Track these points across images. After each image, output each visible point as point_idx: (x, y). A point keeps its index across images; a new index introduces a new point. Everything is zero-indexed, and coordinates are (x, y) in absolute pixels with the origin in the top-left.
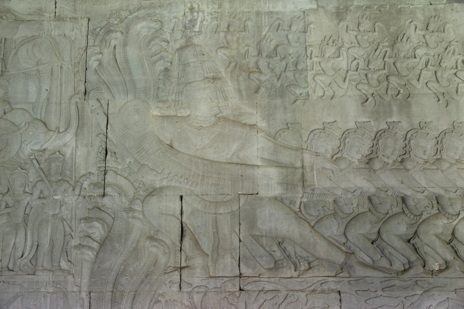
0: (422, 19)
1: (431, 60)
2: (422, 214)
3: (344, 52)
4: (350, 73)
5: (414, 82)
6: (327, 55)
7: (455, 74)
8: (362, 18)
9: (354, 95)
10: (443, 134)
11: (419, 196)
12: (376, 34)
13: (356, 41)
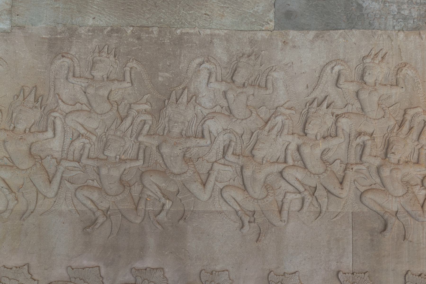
0: (225, 58)
1: (233, 144)
3: (58, 123)
4: (65, 164)
5: (196, 188)
6: (21, 127)
7: (281, 173)
8: (100, 52)
9: (70, 211)
12: (126, 85)
13: (85, 100)
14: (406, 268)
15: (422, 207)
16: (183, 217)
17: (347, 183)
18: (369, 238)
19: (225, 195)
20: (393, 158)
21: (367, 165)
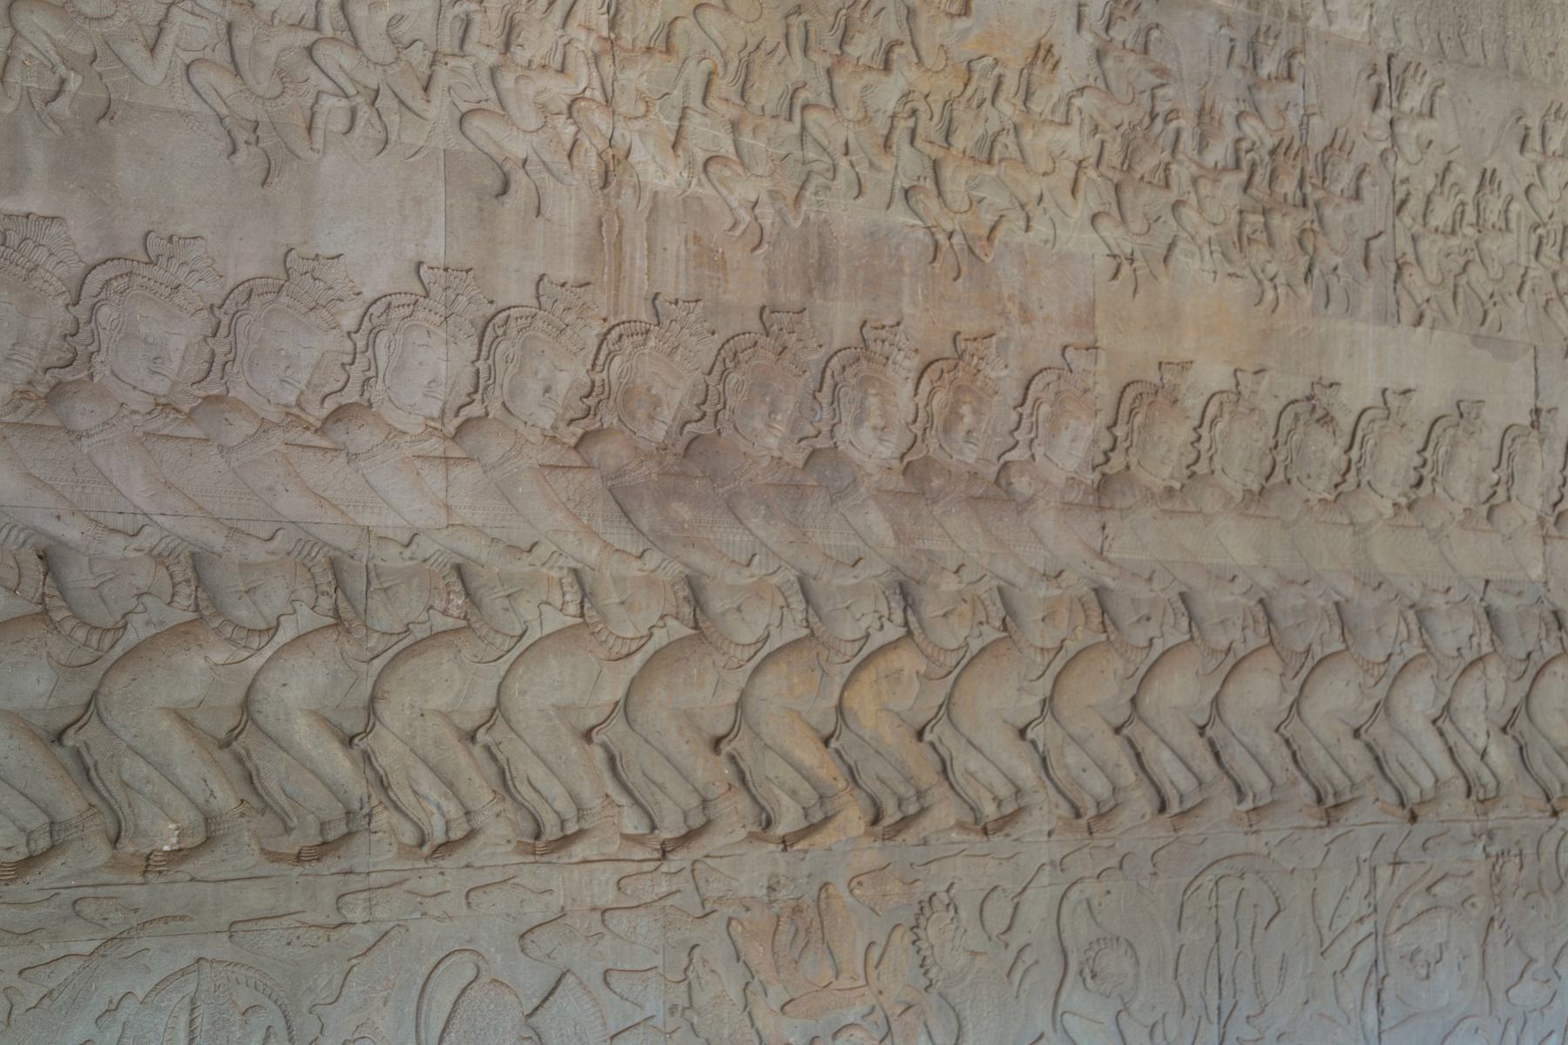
2: (125, 627)
5: (134, 53)
7: (310, 50)
10: (239, 295)
11: (115, 546)
14: (539, 269)
15: (570, 156)
16: (106, 113)
17: (437, 91)
18: (475, 204)
19: (196, 79)
20: (521, 56)
21: (474, 60)
